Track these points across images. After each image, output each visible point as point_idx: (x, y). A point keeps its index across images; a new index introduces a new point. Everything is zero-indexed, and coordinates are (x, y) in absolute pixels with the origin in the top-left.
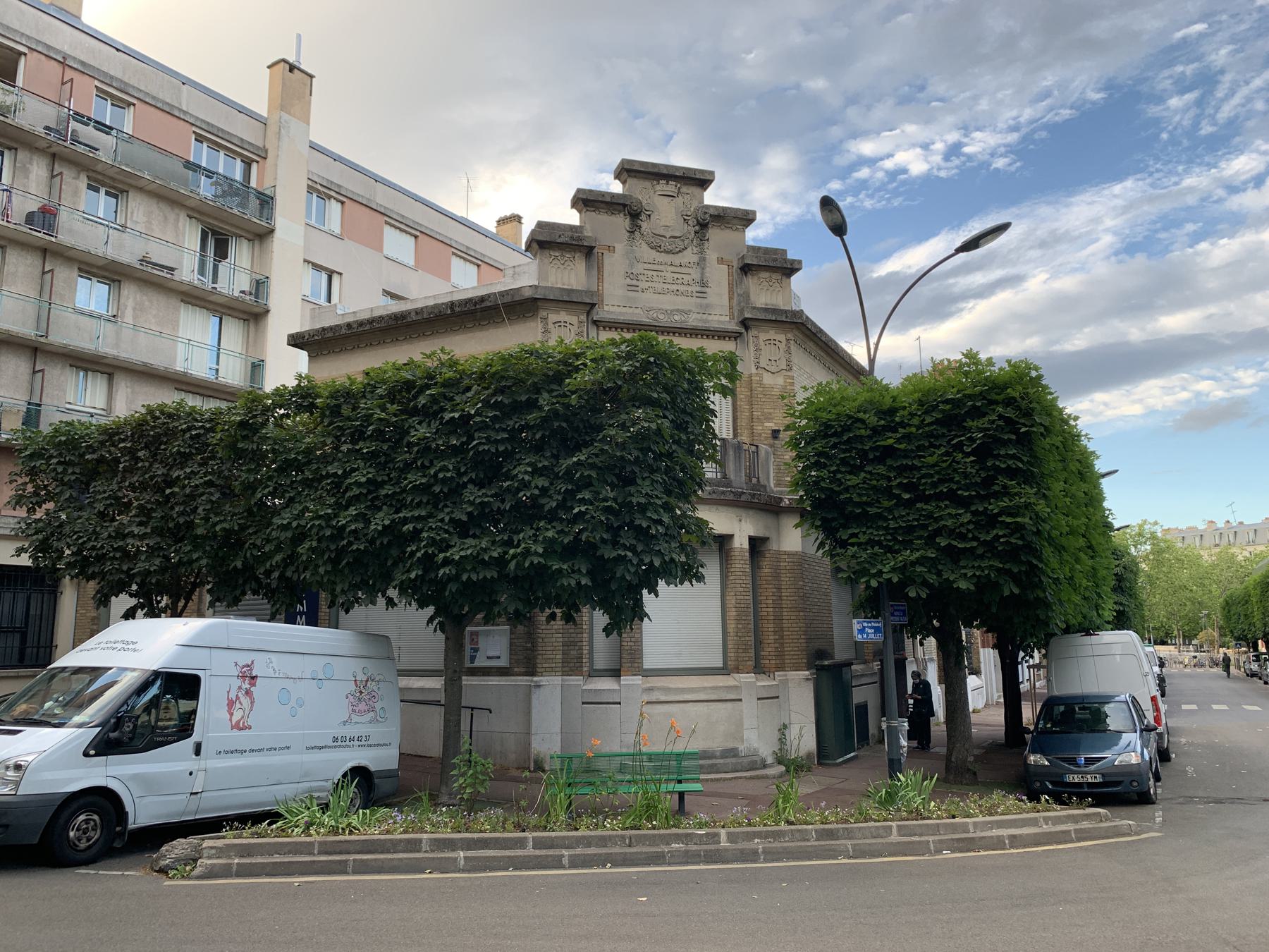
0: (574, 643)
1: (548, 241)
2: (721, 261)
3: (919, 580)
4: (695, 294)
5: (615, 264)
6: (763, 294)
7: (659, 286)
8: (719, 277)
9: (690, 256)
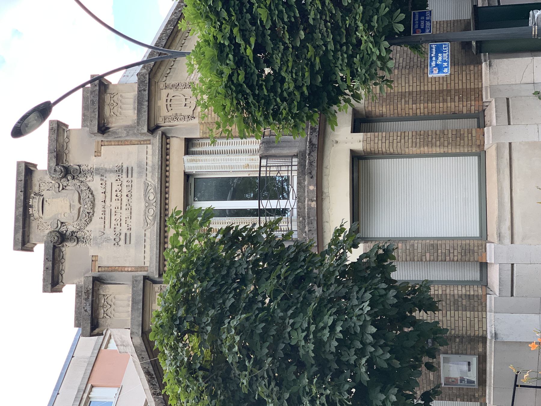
0: (456, 302)
1: (91, 320)
2: (98, 153)
3: (386, 23)
4: (129, 179)
5: (109, 256)
6: (125, 112)
7: (125, 214)
8: (113, 155)
9: (95, 183)
